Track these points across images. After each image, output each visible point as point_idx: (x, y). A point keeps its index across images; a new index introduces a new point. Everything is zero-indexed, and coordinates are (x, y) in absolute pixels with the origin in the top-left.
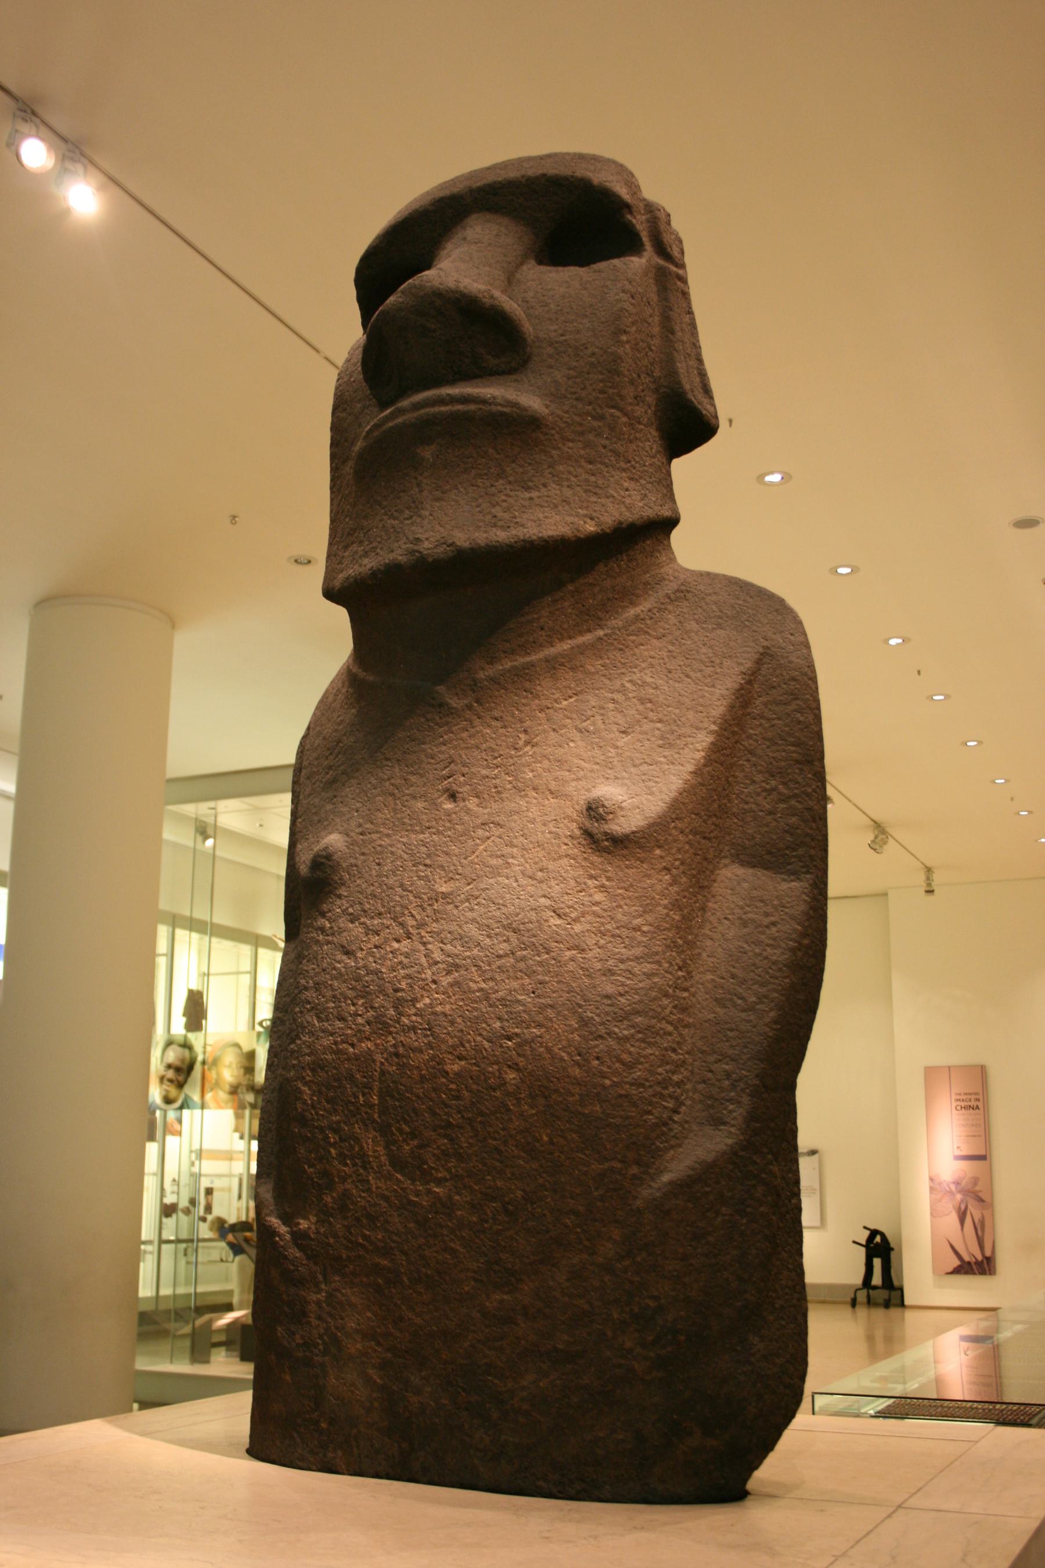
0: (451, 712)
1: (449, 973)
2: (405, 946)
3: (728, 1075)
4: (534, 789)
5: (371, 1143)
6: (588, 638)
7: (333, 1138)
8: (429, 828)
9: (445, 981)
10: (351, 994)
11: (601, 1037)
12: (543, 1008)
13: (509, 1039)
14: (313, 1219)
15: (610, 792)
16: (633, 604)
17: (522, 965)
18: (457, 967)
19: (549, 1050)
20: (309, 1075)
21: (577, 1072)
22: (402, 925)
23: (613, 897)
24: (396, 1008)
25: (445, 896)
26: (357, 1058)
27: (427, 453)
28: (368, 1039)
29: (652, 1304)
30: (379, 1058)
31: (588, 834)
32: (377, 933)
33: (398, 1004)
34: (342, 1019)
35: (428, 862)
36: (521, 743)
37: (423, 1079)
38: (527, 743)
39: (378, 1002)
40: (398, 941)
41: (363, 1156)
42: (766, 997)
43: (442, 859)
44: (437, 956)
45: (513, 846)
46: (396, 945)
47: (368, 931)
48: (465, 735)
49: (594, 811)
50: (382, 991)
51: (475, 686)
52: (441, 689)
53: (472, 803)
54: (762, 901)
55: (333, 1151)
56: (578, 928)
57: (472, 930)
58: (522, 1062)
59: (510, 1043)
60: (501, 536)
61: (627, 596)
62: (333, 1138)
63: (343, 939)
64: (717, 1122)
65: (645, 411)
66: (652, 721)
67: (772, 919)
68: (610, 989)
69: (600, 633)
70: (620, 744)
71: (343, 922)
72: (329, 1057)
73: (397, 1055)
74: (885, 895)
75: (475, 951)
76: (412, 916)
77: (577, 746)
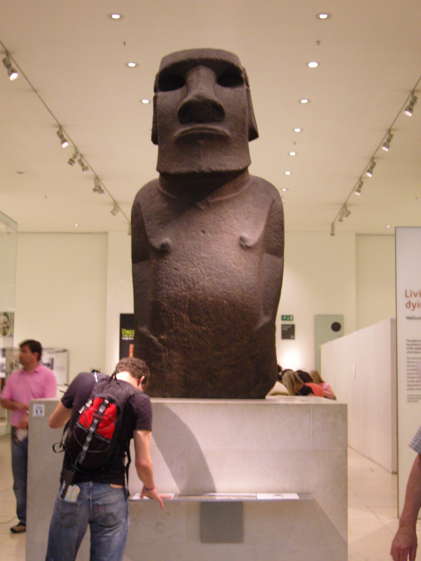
0: (201, 210)
1: (207, 276)
2: (194, 269)
3: (269, 304)
4: (226, 232)
5: (185, 316)
6: (235, 194)
7: (173, 315)
9: (207, 278)
11: (246, 293)
12: (232, 286)
13: (225, 293)
14: (166, 335)
15: (245, 235)
18: (210, 275)
19: (234, 296)
20: (166, 300)
21: (241, 301)
25: (204, 257)
26: (182, 296)
27: (202, 142)
28: (185, 291)
30: (188, 296)
31: (241, 245)
32: (186, 265)
33: (194, 284)
34: (176, 286)
37: (202, 302)
39: (188, 282)
40: (192, 268)
41: (182, 319)
44: (204, 272)
46: (191, 269)
47: (182, 265)
49: (242, 239)
50: (189, 280)
51: (208, 204)
52: (198, 204)
53: (209, 234)
55: (174, 319)
56: (239, 268)
57: (213, 266)
58: (228, 299)
59: (224, 294)
60: (223, 169)
61: (243, 184)
62: (173, 315)
63: (175, 266)
64: (266, 314)
65: (247, 134)
68: (248, 282)
71: (173, 262)
72: (173, 296)
73: (194, 296)
74: (106, 233)
75: (214, 272)
77: (235, 222)
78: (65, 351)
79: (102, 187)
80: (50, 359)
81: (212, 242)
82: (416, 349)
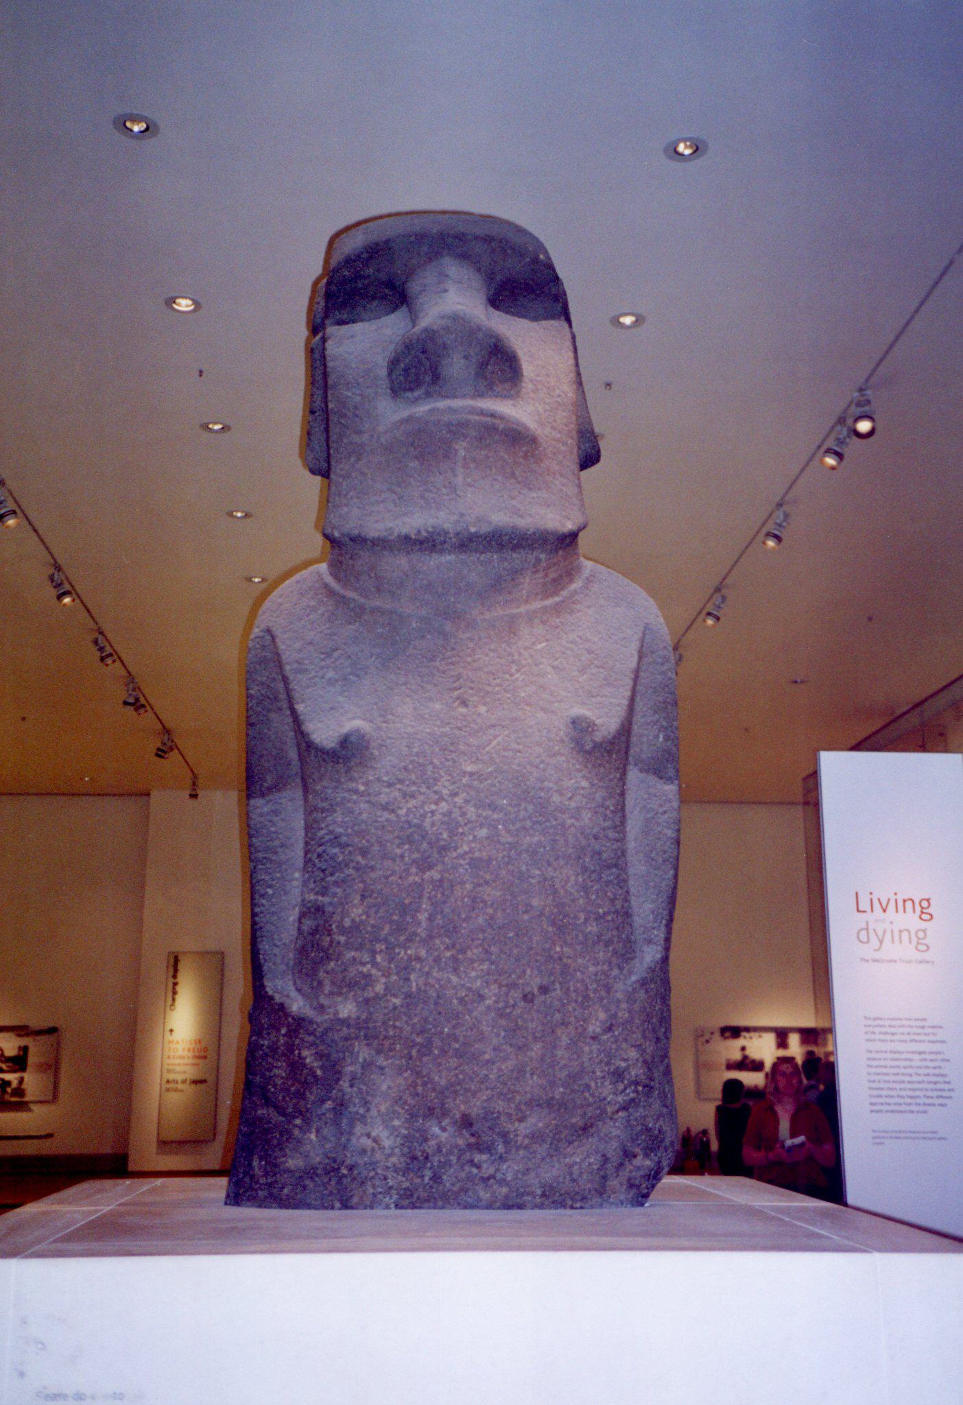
8: (448, 724)
10: (397, 841)
16: (571, 581)
17: (538, 827)
22: (435, 792)
23: (592, 785)
24: (439, 852)
25: (471, 774)
29: (623, 1064)
32: (413, 796)
35: (452, 748)
36: (513, 670)
38: (518, 671)
42: (668, 861)
43: (462, 747)
45: (518, 744)
47: (404, 795)
48: (469, 659)
54: (656, 796)
63: (383, 799)
64: (649, 942)
66: (598, 667)
67: (664, 809)
69: (557, 599)
70: (580, 680)
76: (445, 787)
78: (52, 1030)
79: (143, 701)
80: (20, 1048)
81: (492, 731)
82: (881, 1033)
